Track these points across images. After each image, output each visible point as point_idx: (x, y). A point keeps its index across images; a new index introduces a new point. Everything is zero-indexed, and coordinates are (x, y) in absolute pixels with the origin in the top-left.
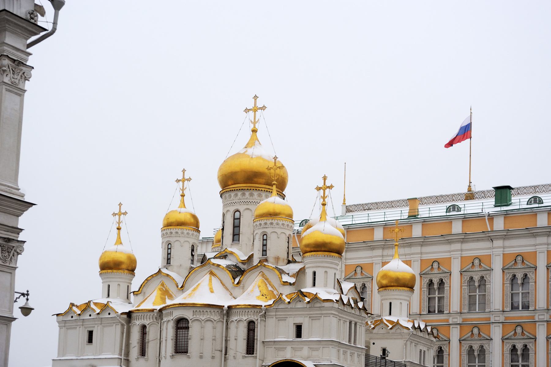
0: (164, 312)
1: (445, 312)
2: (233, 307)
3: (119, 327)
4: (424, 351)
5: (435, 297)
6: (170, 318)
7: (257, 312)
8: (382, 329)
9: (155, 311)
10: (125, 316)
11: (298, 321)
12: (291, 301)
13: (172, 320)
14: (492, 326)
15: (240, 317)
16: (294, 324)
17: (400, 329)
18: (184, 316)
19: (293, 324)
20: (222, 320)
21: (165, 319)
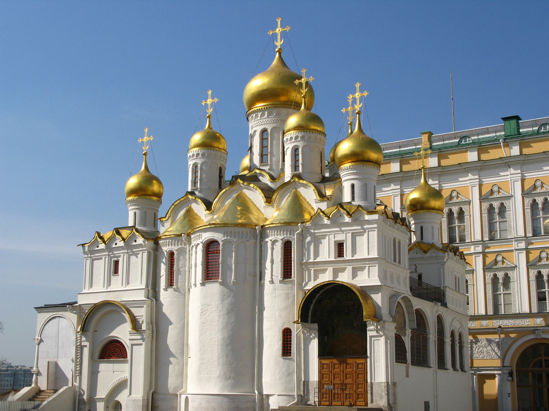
0: (192, 236)
1: (467, 241)
2: (267, 226)
3: (145, 255)
4: (459, 277)
5: (455, 226)
6: (199, 241)
7: (294, 230)
8: (417, 253)
9: (183, 235)
10: (151, 243)
11: (340, 237)
12: (330, 216)
13: (202, 243)
14: (515, 253)
15: (274, 236)
16: (335, 241)
17: (435, 253)
18: (214, 238)
19: (333, 242)
20: (255, 241)
21: (194, 243)
